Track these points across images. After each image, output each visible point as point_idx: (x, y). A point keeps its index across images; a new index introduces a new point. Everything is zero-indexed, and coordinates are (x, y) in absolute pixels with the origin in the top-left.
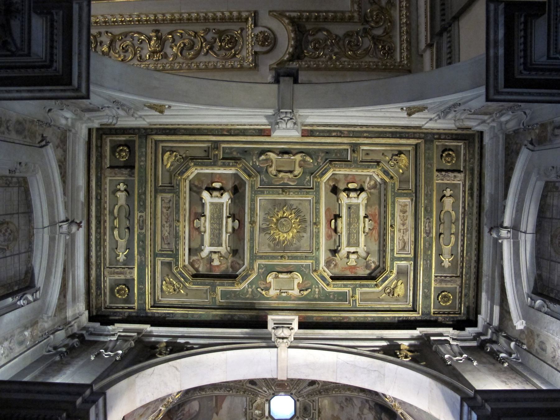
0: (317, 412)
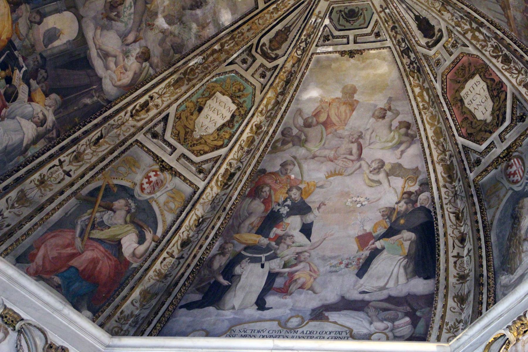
0: (352, 46)
